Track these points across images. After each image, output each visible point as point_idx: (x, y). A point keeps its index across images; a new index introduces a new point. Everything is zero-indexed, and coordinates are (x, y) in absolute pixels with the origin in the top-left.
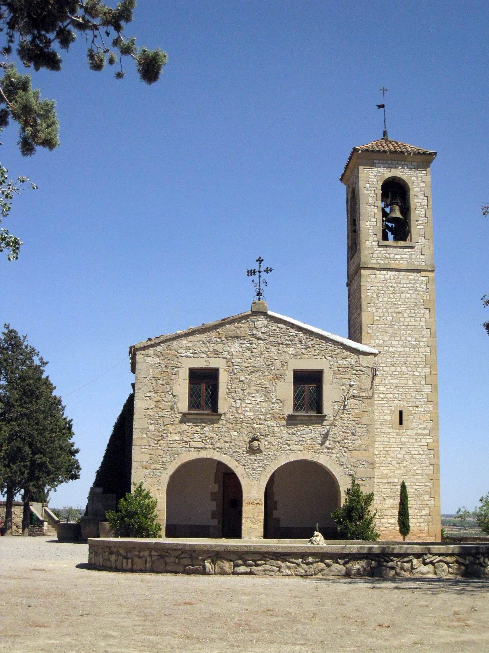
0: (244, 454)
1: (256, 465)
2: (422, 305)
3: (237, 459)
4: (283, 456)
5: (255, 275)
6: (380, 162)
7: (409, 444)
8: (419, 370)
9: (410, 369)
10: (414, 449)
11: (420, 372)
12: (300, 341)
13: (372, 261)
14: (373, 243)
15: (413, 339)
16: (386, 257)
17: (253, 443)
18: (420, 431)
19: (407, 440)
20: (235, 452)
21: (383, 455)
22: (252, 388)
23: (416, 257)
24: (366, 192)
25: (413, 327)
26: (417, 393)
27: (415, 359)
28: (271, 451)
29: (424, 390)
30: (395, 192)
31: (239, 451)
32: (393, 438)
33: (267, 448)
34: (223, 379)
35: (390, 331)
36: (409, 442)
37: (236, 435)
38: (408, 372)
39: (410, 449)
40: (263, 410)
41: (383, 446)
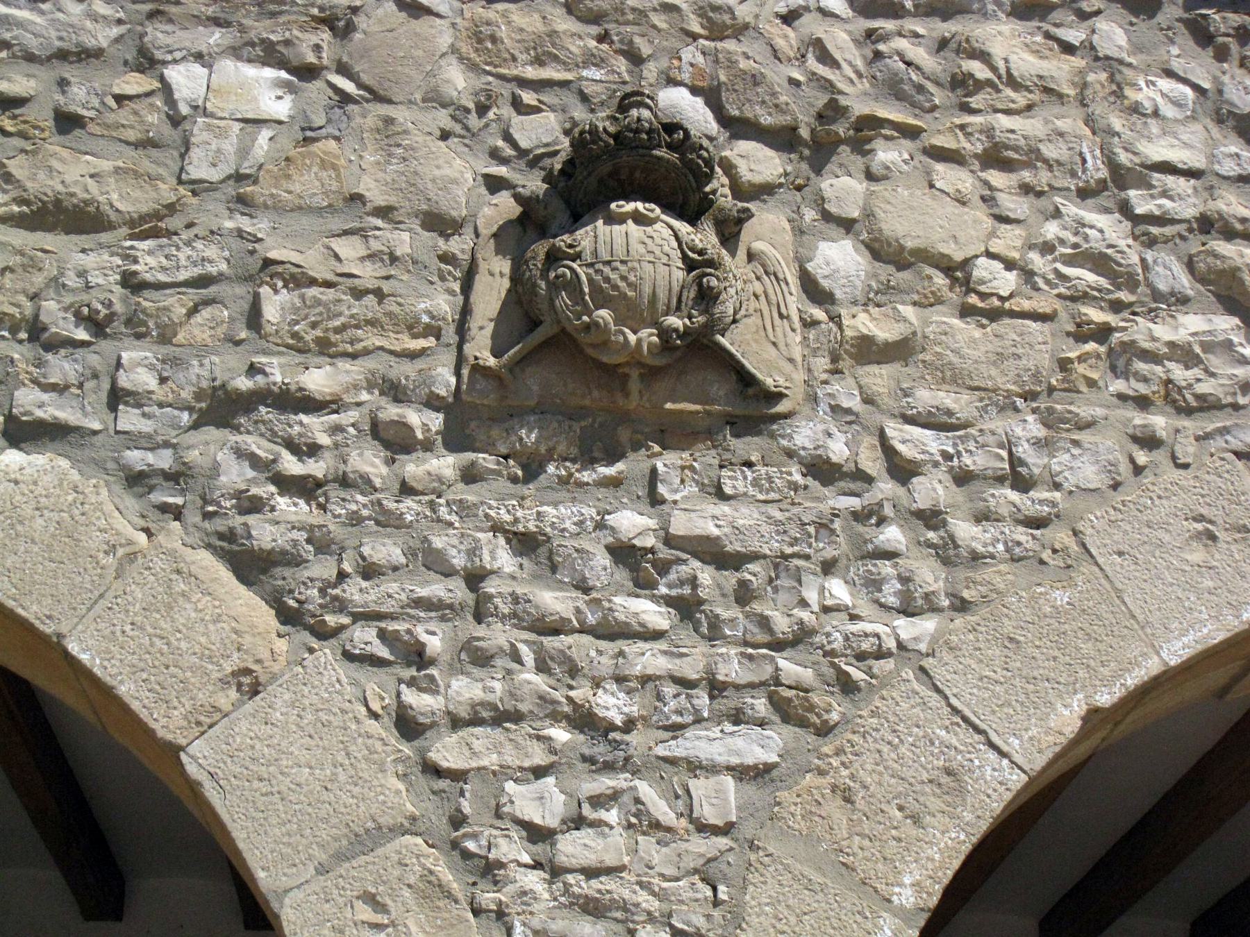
0: (397, 442)
1: (648, 659)
3: (264, 534)
4: (1169, 495)
17: (594, 236)
20: (222, 408)
28: (926, 397)
31: (318, 379)
33: (868, 351)
37: (281, 108)
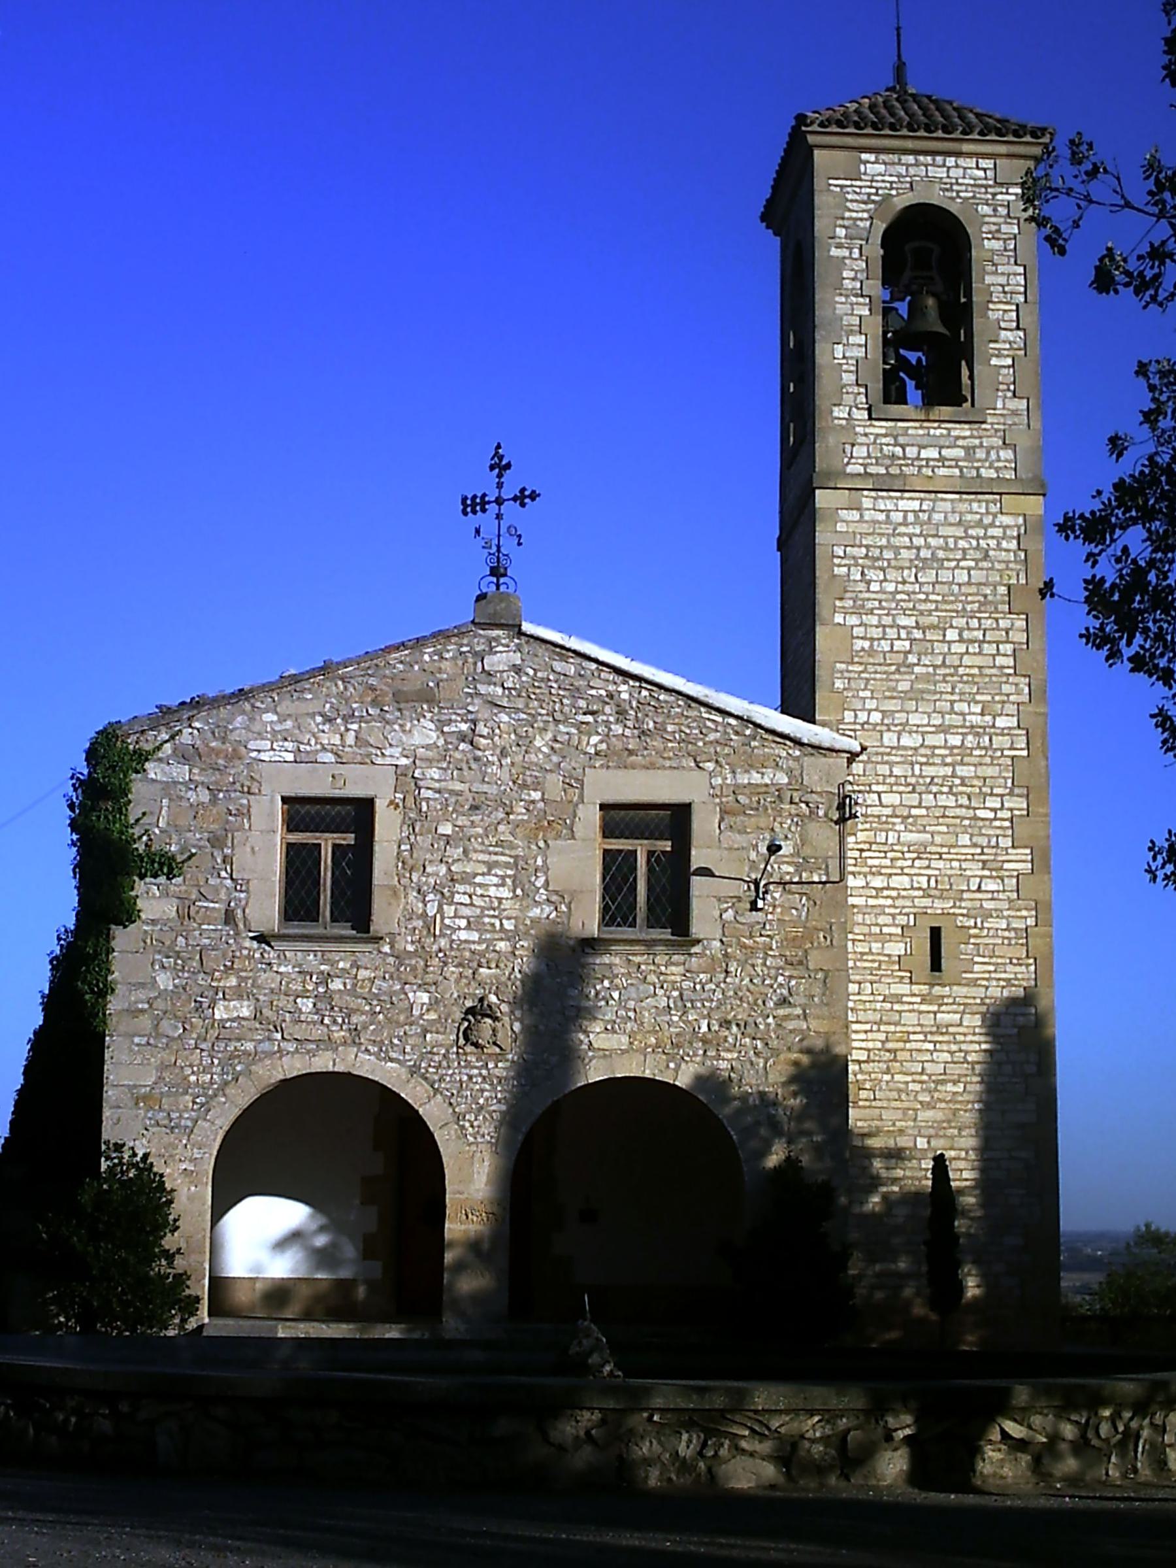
2: (1003, 603)
5: (484, 510)
6: (882, 157)
7: (961, 1030)
8: (994, 803)
9: (964, 801)
11: (995, 810)
12: (621, 713)
13: (849, 469)
14: (857, 415)
15: (977, 709)
16: (893, 456)
22: (474, 856)
23: (988, 453)
24: (834, 252)
25: (976, 671)
26: (987, 873)
27: (981, 771)
30: (927, 249)
32: (910, 1011)
34: (387, 828)
35: (904, 686)
36: (960, 1025)
39: (964, 1047)
40: (509, 925)
41: (882, 1037)
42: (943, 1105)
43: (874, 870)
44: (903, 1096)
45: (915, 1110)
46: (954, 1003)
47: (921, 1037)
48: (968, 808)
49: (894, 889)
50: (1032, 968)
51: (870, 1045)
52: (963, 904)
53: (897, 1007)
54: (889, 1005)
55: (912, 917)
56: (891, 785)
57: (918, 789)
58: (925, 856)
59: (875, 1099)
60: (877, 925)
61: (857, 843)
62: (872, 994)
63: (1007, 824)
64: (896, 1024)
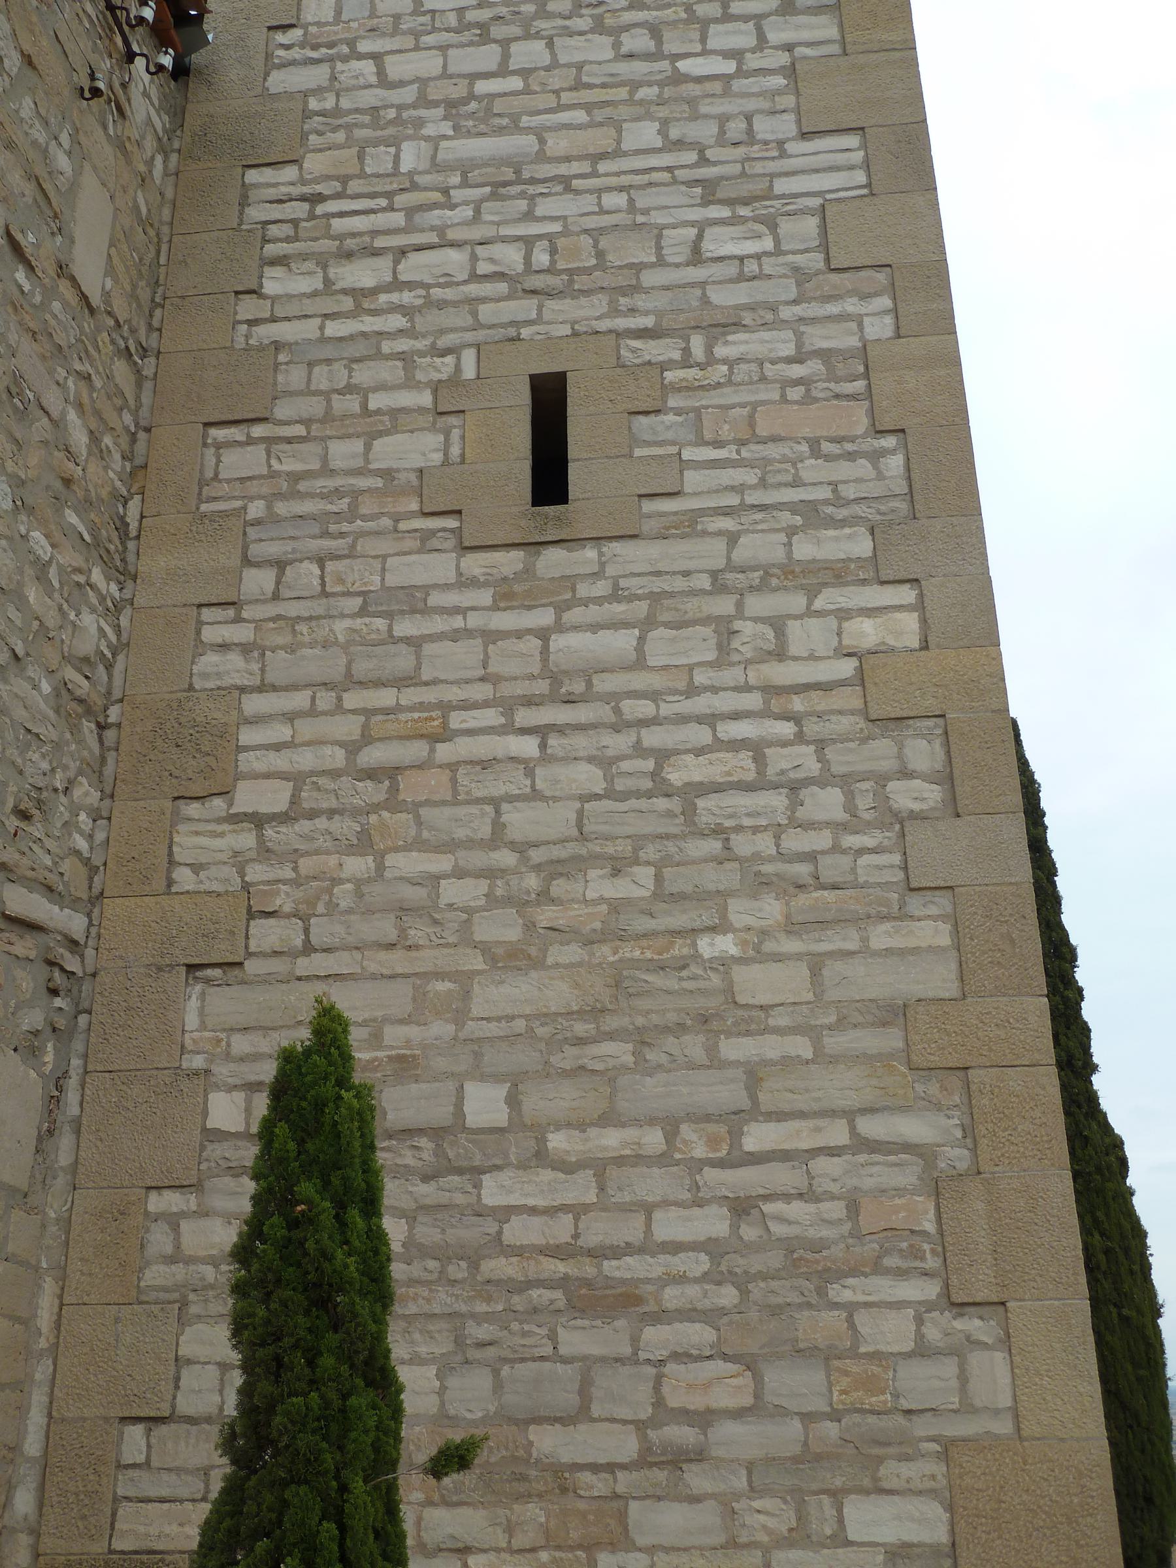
7: (639, 681)
9: (639, 41)
10: (701, 735)
11: (736, 54)
18: (763, 547)
19: (623, 642)
21: (346, 827)
29: (782, 186)
32: (455, 636)
36: (640, 663)
38: (625, 69)
39: (653, 738)
41: (349, 728)
42: (572, 953)
43: (350, 243)
44: (418, 933)
45: (464, 979)
46: (615, 596)
47: (491, 717)
48: (654, 56)
49: (410, 285)
50: (895, 463)
51: (305, 760)
52: (640, 301)
53: (405, 627)
54: (380, 623)
55: (469, 357)
56: (417, 34)
57: (497, 31)
58: (514, 190)
59: (308, 948)
60: (350, 389)
61: (303, 182)
62: (325, 594)
63: (779, 81)
64: (401, 682)
